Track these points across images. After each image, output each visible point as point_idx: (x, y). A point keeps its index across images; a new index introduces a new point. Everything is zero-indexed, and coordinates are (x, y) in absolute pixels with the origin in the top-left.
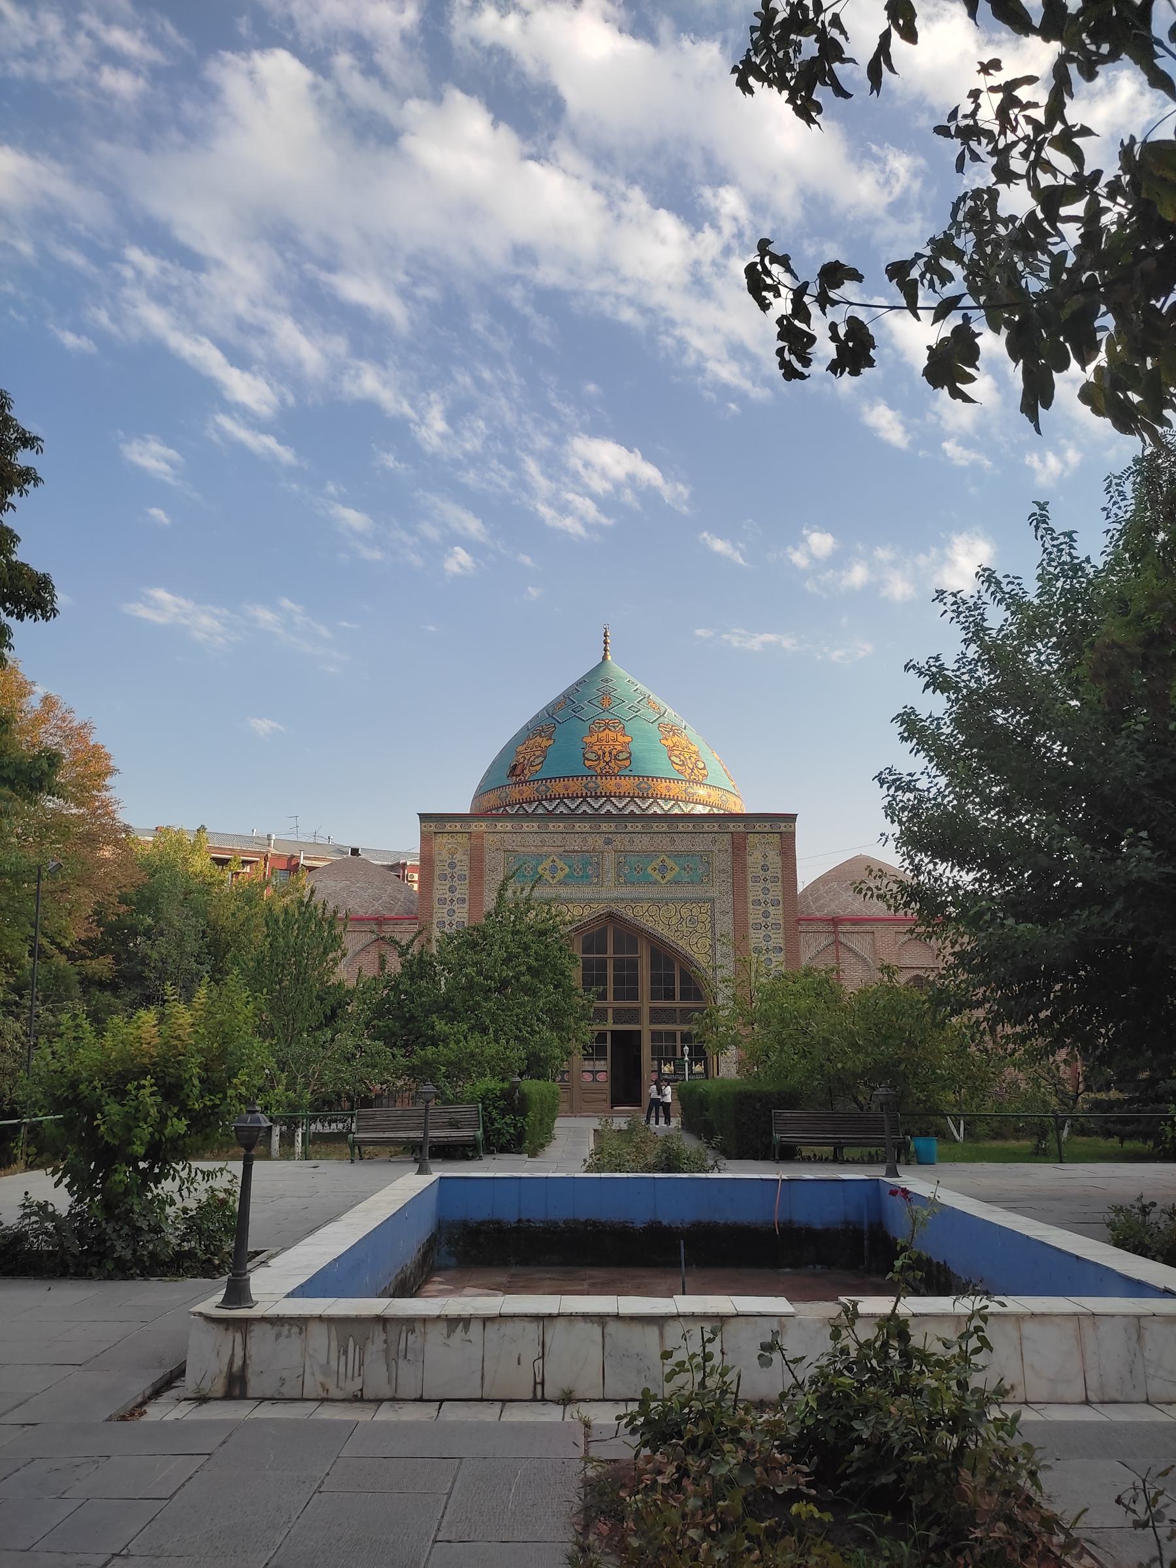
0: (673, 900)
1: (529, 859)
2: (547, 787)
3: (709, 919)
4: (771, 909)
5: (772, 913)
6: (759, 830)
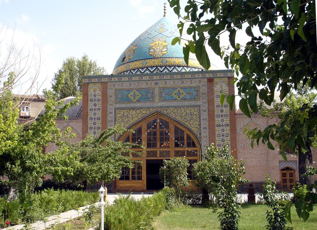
0: (183, 107)
1: (125, 92)
3: (198, 114)
4: (224, 109)
6: (219, 76)
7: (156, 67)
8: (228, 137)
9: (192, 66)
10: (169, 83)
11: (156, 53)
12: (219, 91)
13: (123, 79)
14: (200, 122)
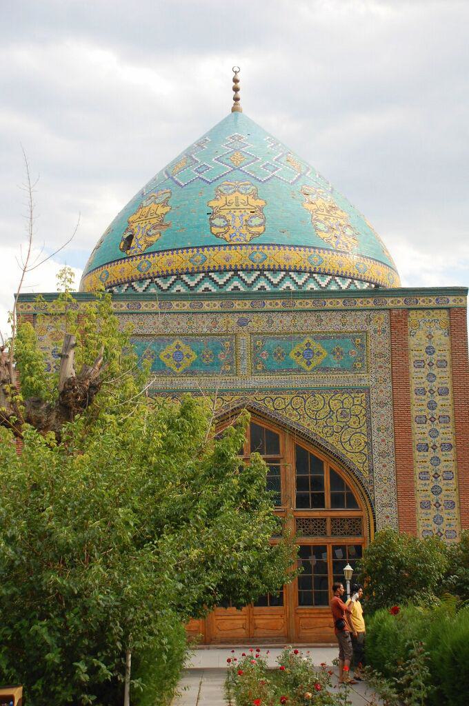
0: (320, 390)
3: (364, 412)
4: (438, 399)
7: (232, 273)
8: (450, 482)
9: (348, 275)
10: (281, 322)
11: (232, 231)
13: (143, 306)
14: (369, 434)
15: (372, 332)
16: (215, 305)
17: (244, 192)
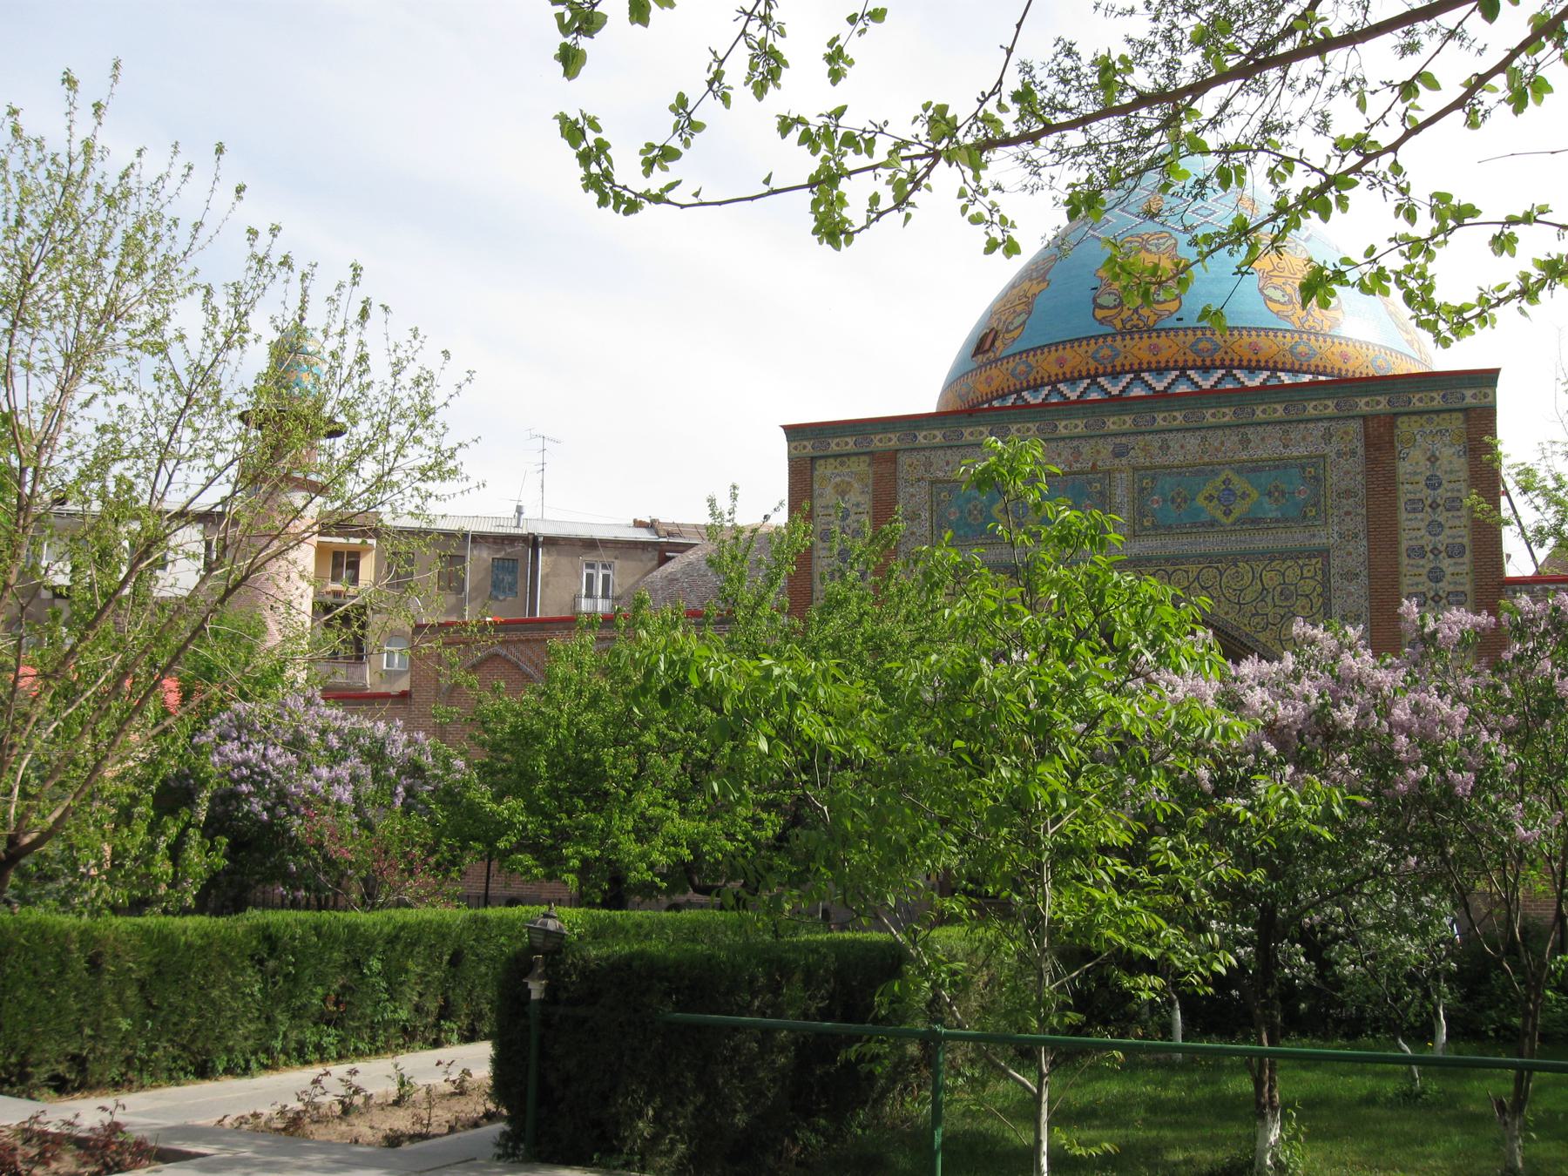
0: (1248, 556)
2: (1030, 366)
3: (1319, 589)
4: (1446, 564)
5: (1449, 571)
6: (1419, 406)
12: (1422, 479)
15: (1333, 456)
16: (1076, 426)
17: (1154, 249)
